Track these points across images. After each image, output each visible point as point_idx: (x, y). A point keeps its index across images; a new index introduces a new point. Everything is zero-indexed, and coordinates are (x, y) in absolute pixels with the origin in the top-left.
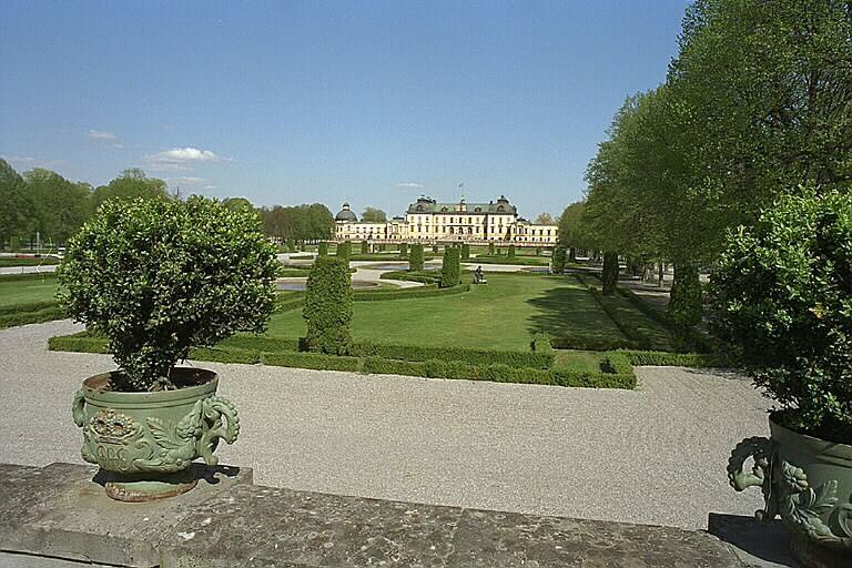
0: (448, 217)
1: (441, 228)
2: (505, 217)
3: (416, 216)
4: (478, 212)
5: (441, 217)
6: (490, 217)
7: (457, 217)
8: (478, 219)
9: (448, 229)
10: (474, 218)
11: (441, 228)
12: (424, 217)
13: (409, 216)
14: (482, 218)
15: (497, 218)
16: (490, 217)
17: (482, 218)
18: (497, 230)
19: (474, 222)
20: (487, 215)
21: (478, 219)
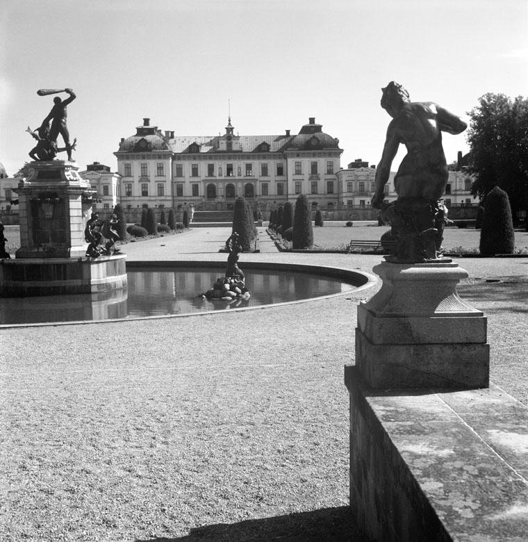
1: (188, 190)
2: (322, 163)
3: (136, 166)
12: (152, 165)
14: (272, 165)
15: (306, 163)
16: (291, 163)
17: (272, 165)
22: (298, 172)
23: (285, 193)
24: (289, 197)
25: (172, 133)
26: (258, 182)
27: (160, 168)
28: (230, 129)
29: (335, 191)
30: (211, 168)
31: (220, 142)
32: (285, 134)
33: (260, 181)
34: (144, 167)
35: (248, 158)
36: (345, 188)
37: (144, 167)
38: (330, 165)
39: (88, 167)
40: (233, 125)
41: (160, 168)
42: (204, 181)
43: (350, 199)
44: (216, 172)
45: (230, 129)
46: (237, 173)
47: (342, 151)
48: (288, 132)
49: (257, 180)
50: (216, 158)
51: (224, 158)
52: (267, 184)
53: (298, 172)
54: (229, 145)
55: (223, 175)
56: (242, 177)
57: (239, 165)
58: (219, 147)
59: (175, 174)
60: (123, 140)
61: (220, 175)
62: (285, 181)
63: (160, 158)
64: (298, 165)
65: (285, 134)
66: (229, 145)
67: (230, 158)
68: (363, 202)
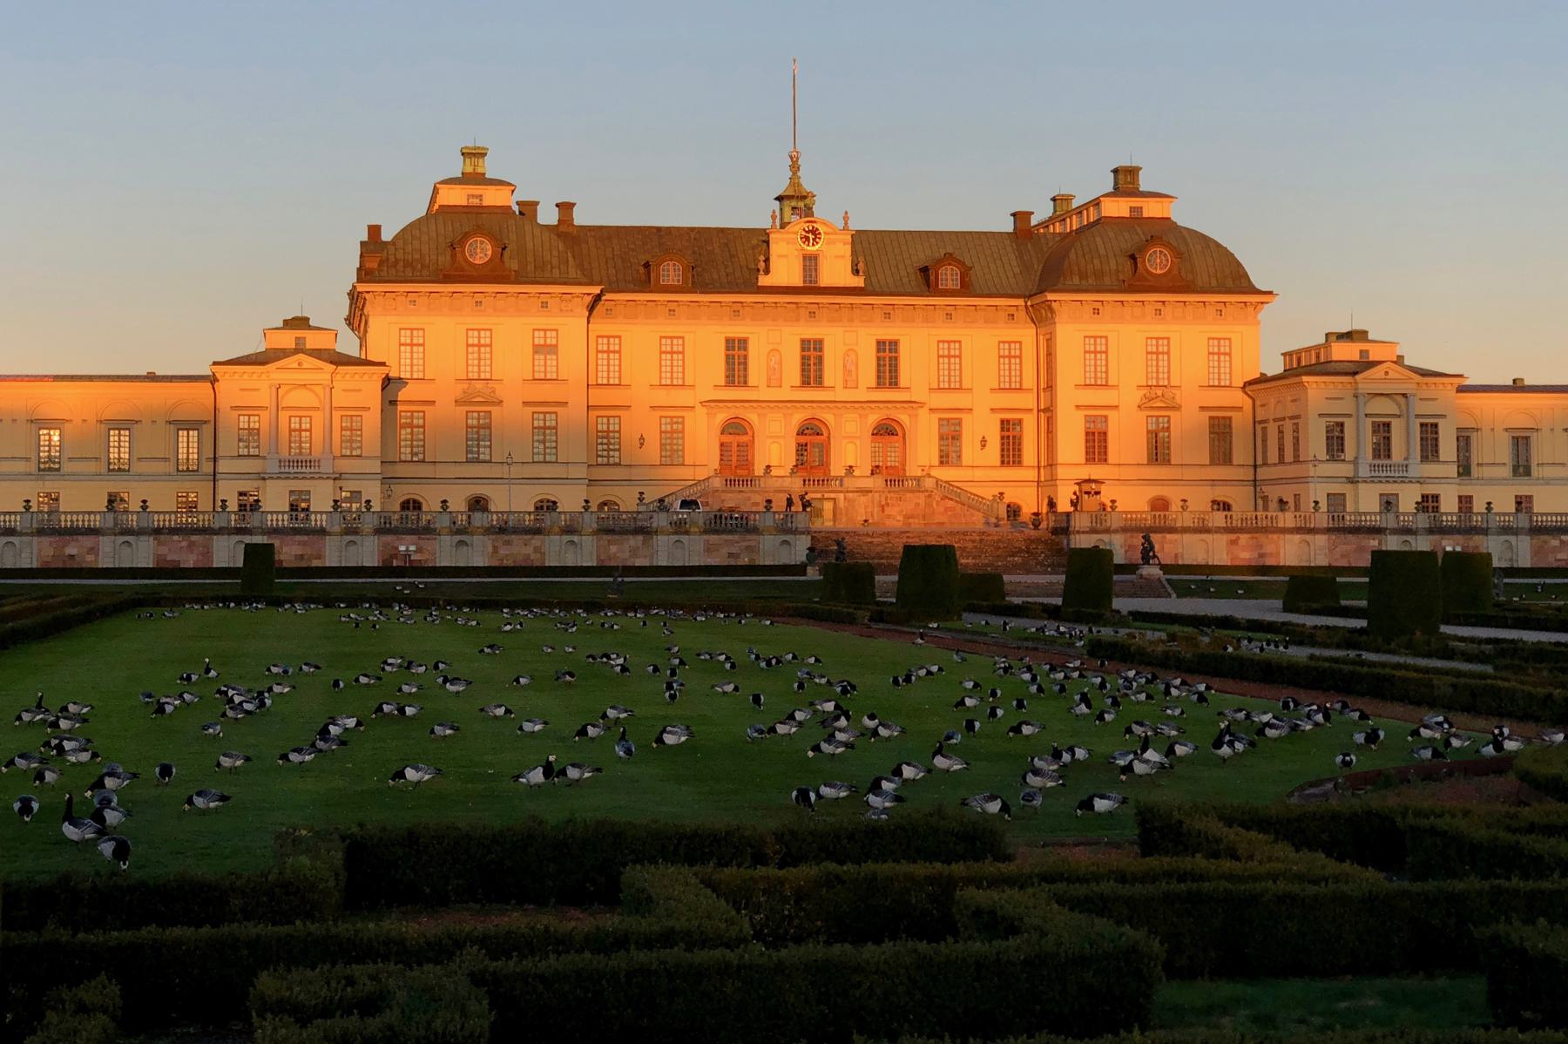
7: (774, 342)
8: (950, 354)
21: (950, 354)
25: (565, 208)
26: (923, 413)
28: (795, 200)
30: (736, 352)
32: (1008, 226)
36: (1316, 443)
38: (1220, 351)
39: (286, 322)
40: (807, 185)
43: (1336, 488)
45: (795, 200)
46: (840, 375)
47: (1270, 293)
48: (1020, 217)
52: (959, 422)
54: (811, 263)
55: (786, 384)
56: (861, 395)
57: (850, 343)
58: (767, 271)
60: (374, 231)
61: (774, 381)
64: (1097, 350)
65: (1008, 226)
66: (811, 263)
68: (1388, 503)
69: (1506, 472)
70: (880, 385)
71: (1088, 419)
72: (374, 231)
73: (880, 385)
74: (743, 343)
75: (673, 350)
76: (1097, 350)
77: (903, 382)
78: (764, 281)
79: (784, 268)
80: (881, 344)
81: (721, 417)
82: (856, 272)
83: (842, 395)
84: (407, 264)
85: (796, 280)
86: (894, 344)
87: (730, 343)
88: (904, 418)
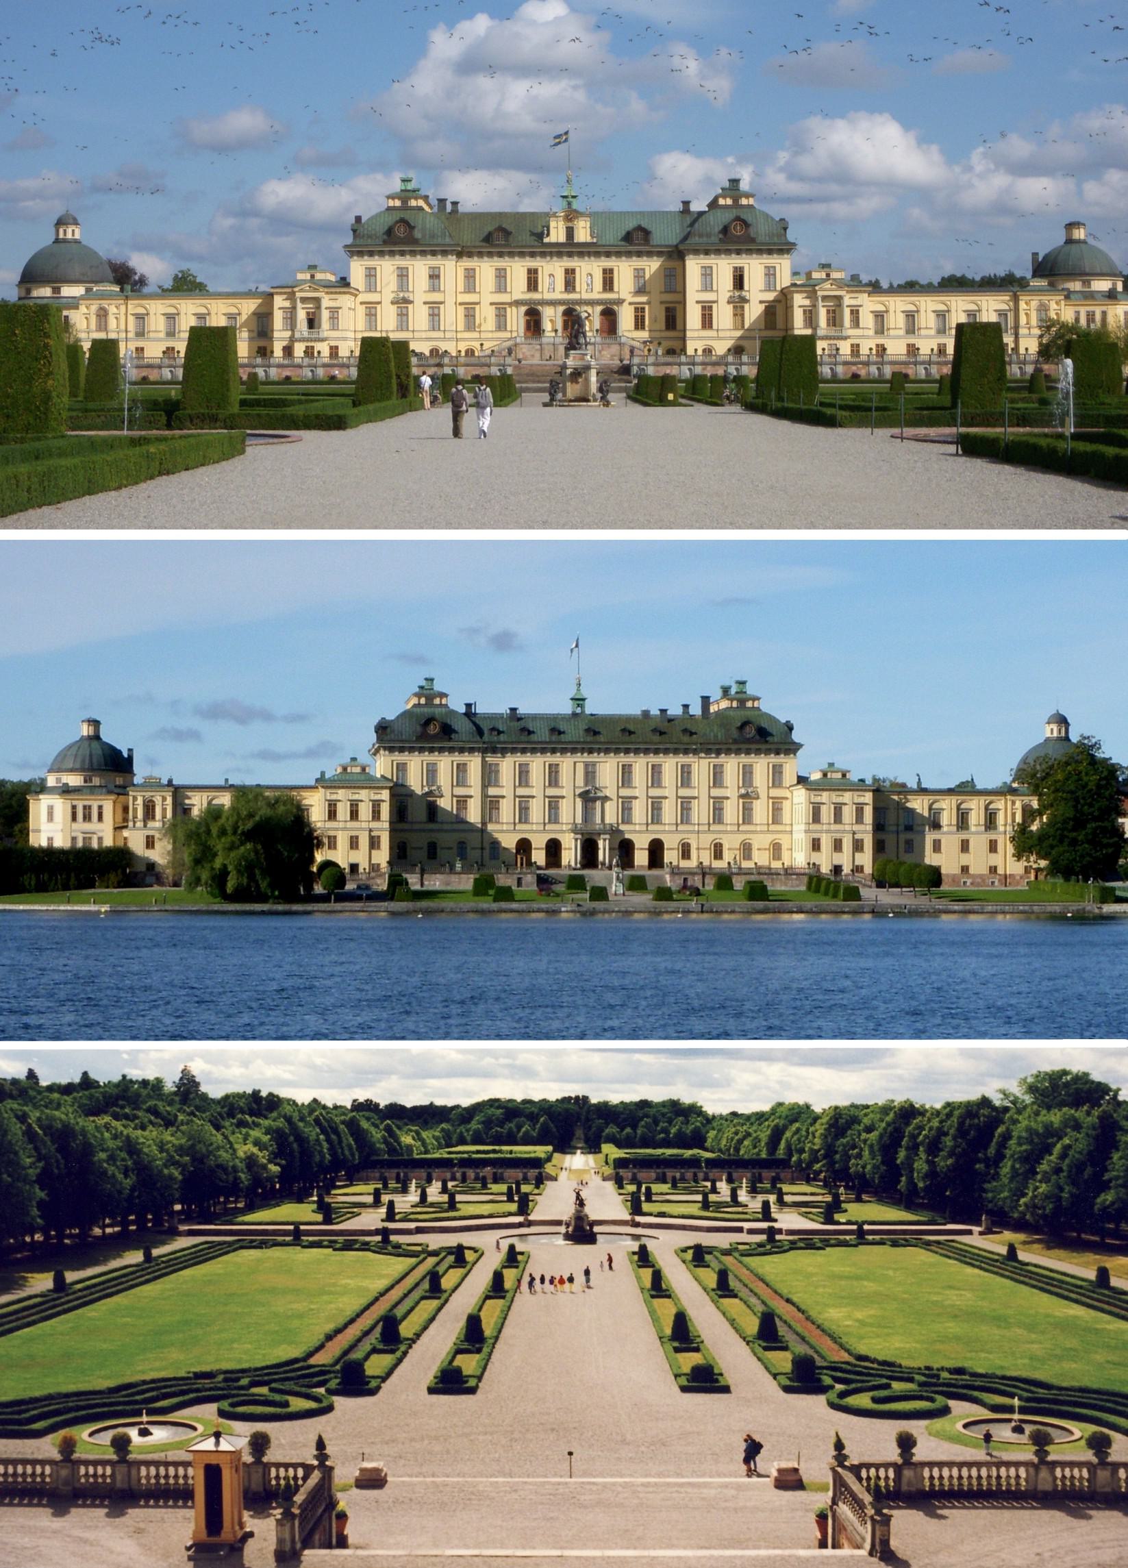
0: (517, 269)
1: (486, 316)
2: (755, 267)
3: (387, 267)
4: (636, 240)
5: (486, 269)
6: (693, 266)
7: (552, 270)
9: (516, 320)
10: (625, 271)
11: (486, 316)
12: (419, 267)
13: (357, 270)
15: (724, 267)
18: (724, 315)
19: (625, 284)
20: (676, 255)
22: (707, 286)
23: (679, 326)
24: (689, 334)
26: (625, 304)
27: (434, 276)
29: (780, 324)
31: (553, 224)
33: (630, 304)
34: (403, 275)
35: (608, 255)
37: (403, 275)
38: (770, 273)
41: (434, 276)
42: (517, 303)
44: (543, 281)
46: (585, 286)
47: (794, 244)
49: (624, 301)
50: (543, 255)
51: (560, 255)
53: (707, 286)
54: (570, 232)
57: (589, 270)
58: (548, 235)
59: (461, 288)
60: (358, 219)
62: (679, 303)
63: (434, 253)
64: (707, 273)
66: (570, 232)
67: (570, 255)
69: (902, 332)
70: (605, 290)
71: (704, 308)
72: (358, 219)
73: (605, 290)
74: (536, 271)
75: (501, 275)
76: (707, 273)
77: (616, 289)
78: (546, 240)
79: (557, 234)
80: (605, 271)
81: (523, 309)
82: (592, 237)
83: (585, 296)
84: (370, 237)
85: (562, 238)
86: (611, 271)
87: (529, 271)
88: (615, 307)
